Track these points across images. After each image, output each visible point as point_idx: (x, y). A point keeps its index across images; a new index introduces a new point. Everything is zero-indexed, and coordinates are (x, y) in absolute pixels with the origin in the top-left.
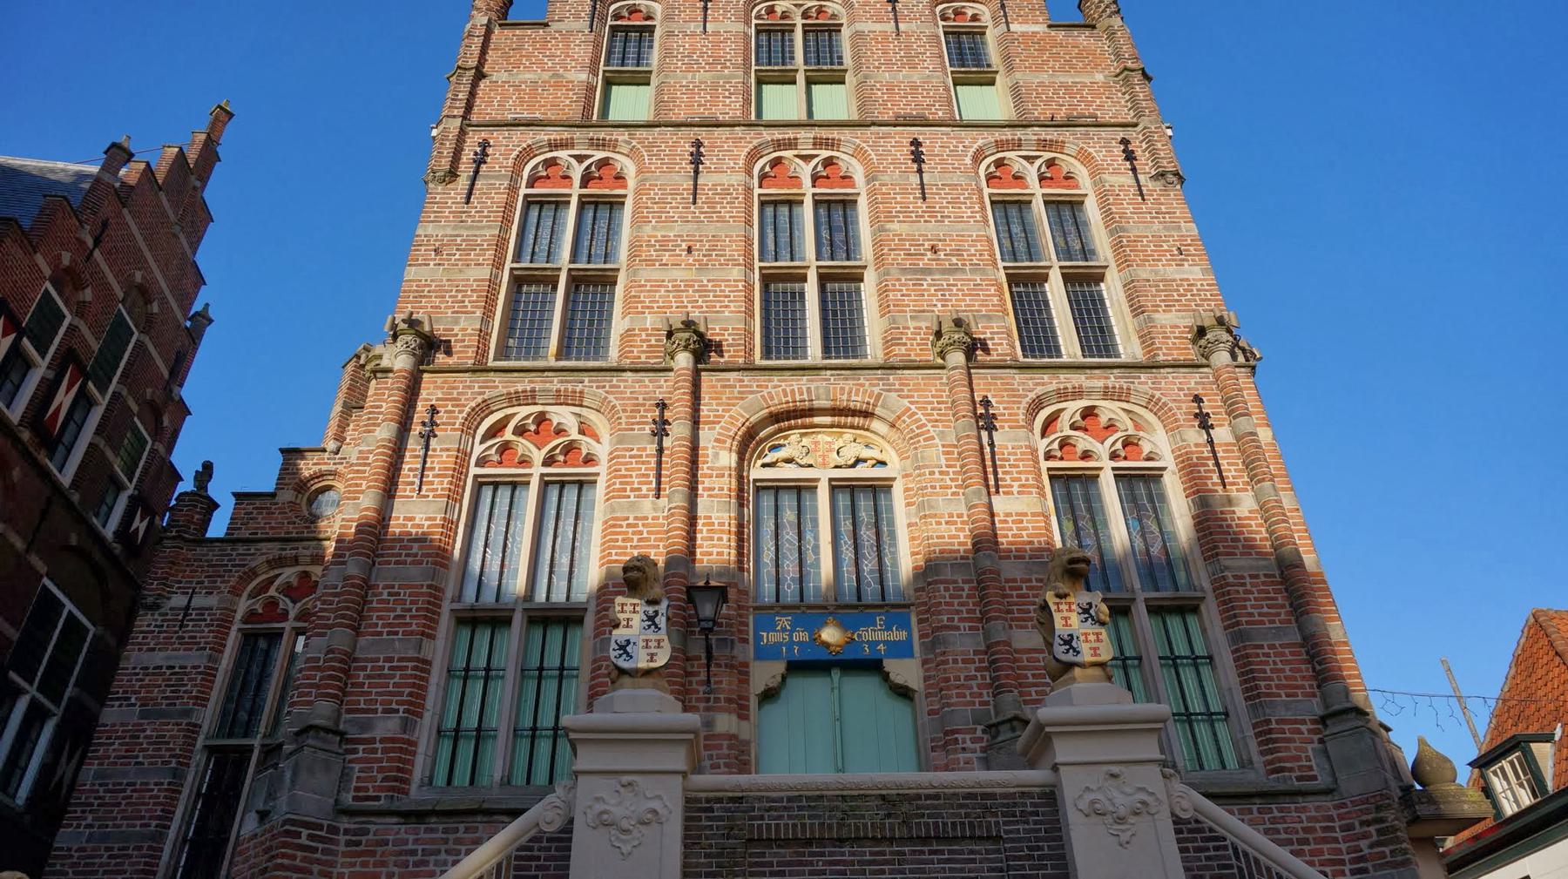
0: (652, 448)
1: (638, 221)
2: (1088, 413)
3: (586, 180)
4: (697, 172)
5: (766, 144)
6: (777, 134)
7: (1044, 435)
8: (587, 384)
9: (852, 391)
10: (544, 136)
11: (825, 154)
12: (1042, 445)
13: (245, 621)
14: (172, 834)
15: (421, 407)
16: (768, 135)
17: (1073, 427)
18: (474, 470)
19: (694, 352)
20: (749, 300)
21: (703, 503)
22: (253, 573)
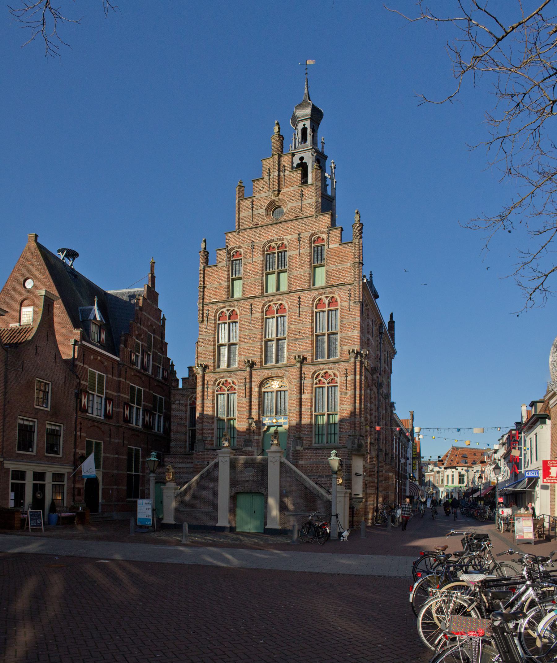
0: (244, 388)
1: (240, 330)
2: (326, 373)
3: (230, 316)
4: (251, 314)
5: (266, 302)
6: (268, 299)
7: (316, 378)
8: (233, 374)
9: (279, 372)
10: (221, 305)
11: (280, 302)
12: (315, 381)
13: (190, 405)
14: (187, 444)
15: (206, 381)
16: (267, 299)
17: (322, 377)
18: (216, 393)
19: (250, 367)
20: (262, 350)
21: (253, 398)
22: (188, 396)
